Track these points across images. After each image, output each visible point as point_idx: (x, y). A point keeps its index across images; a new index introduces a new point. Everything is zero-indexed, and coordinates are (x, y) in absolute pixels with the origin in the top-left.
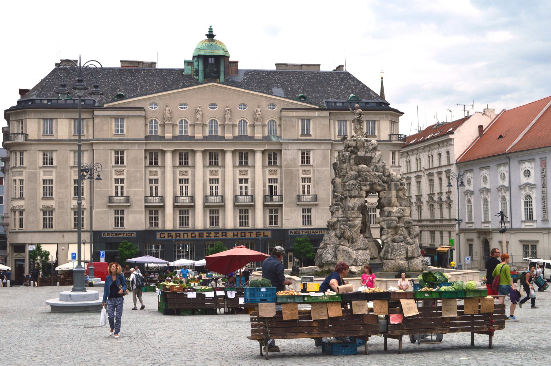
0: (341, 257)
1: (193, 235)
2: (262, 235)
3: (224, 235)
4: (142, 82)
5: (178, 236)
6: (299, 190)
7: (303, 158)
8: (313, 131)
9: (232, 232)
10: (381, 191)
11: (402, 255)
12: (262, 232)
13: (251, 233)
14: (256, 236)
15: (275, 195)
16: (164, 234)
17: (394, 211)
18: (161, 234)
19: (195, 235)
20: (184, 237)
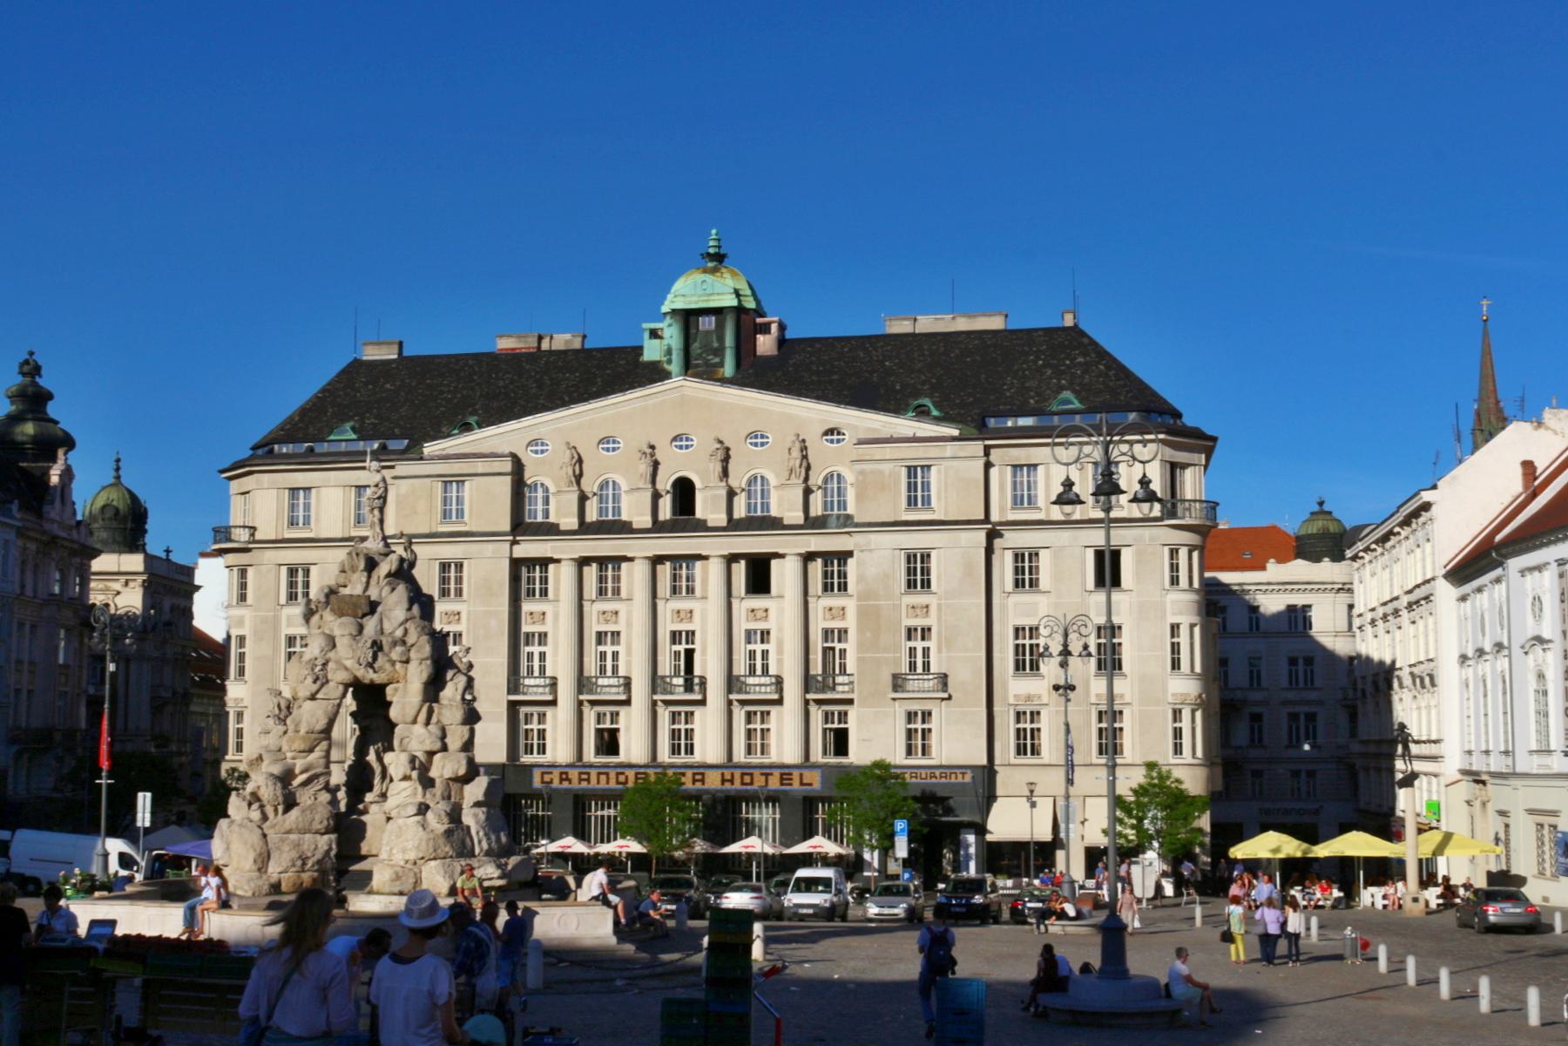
1: (622, 778)
2: (796, 785)
3: (698, 780)
4: (532, 388)
5: (584, 780)
6: (897, 661)
7: (911, 572)
8: (939, 499)
9: (720, 771)
12: (796, 773)
13: (767, 775)
14: (782, 784)
15: (840, 674)
16: (551, 773)
18: (543, 774)
19: (627, 777)
20: (598, 782)
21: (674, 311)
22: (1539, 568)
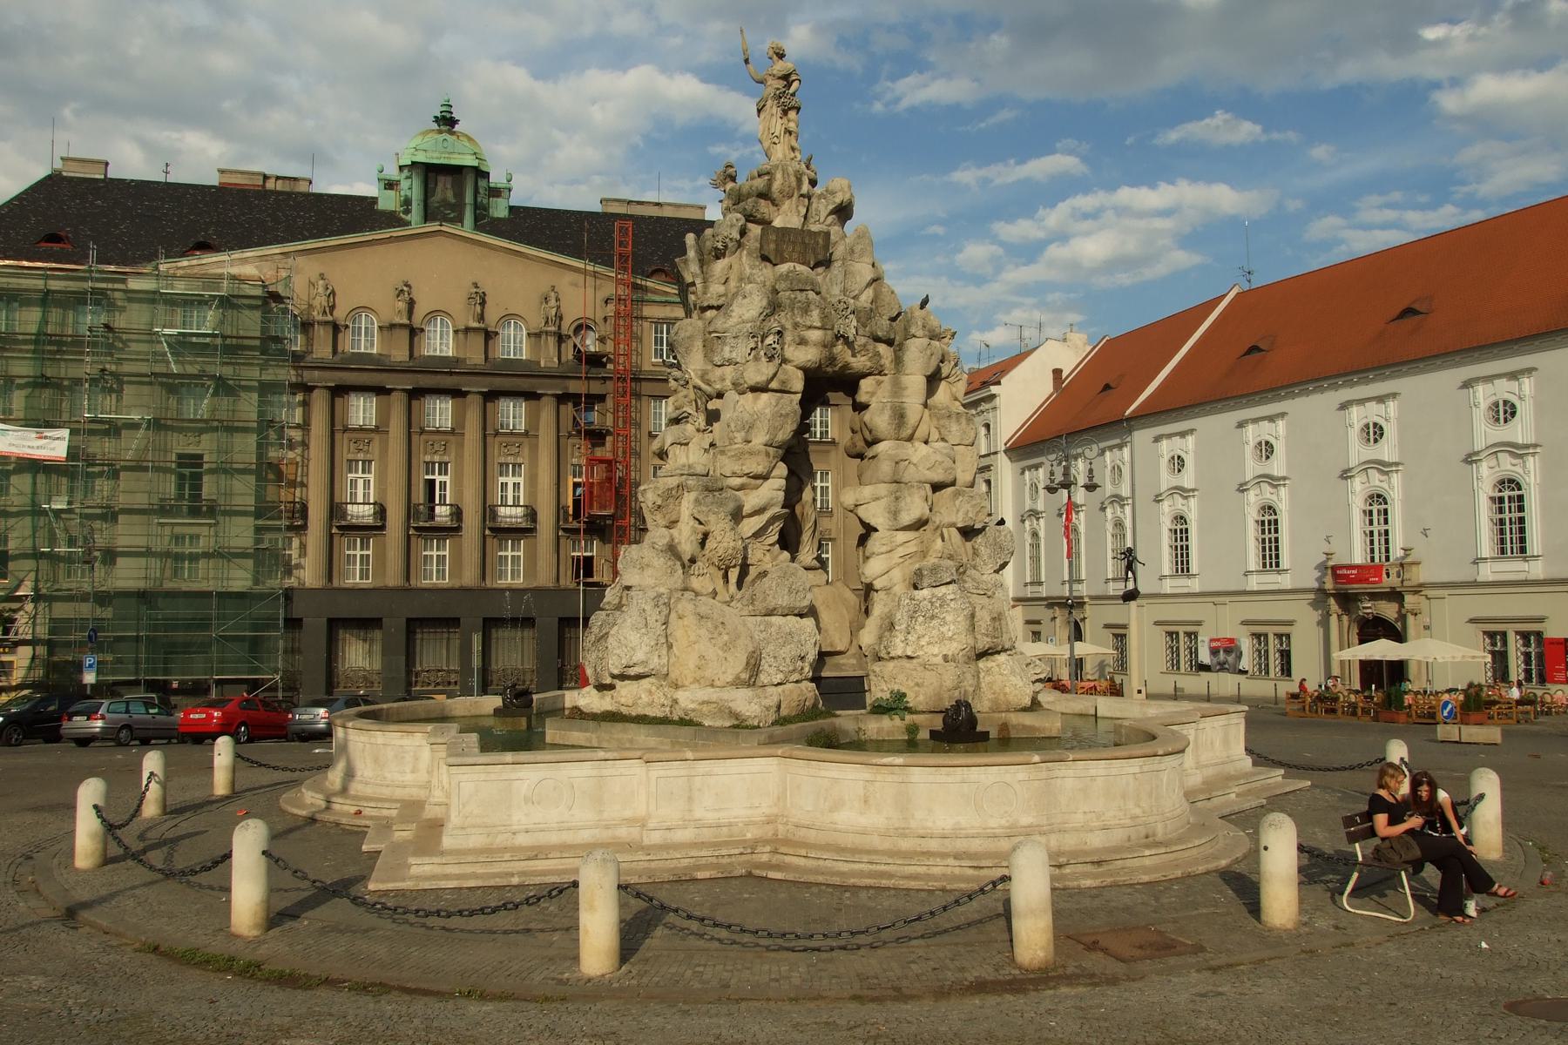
10: (865, 376)
11: (951, 639)
21: (414, 163)
22: (1183, 434)
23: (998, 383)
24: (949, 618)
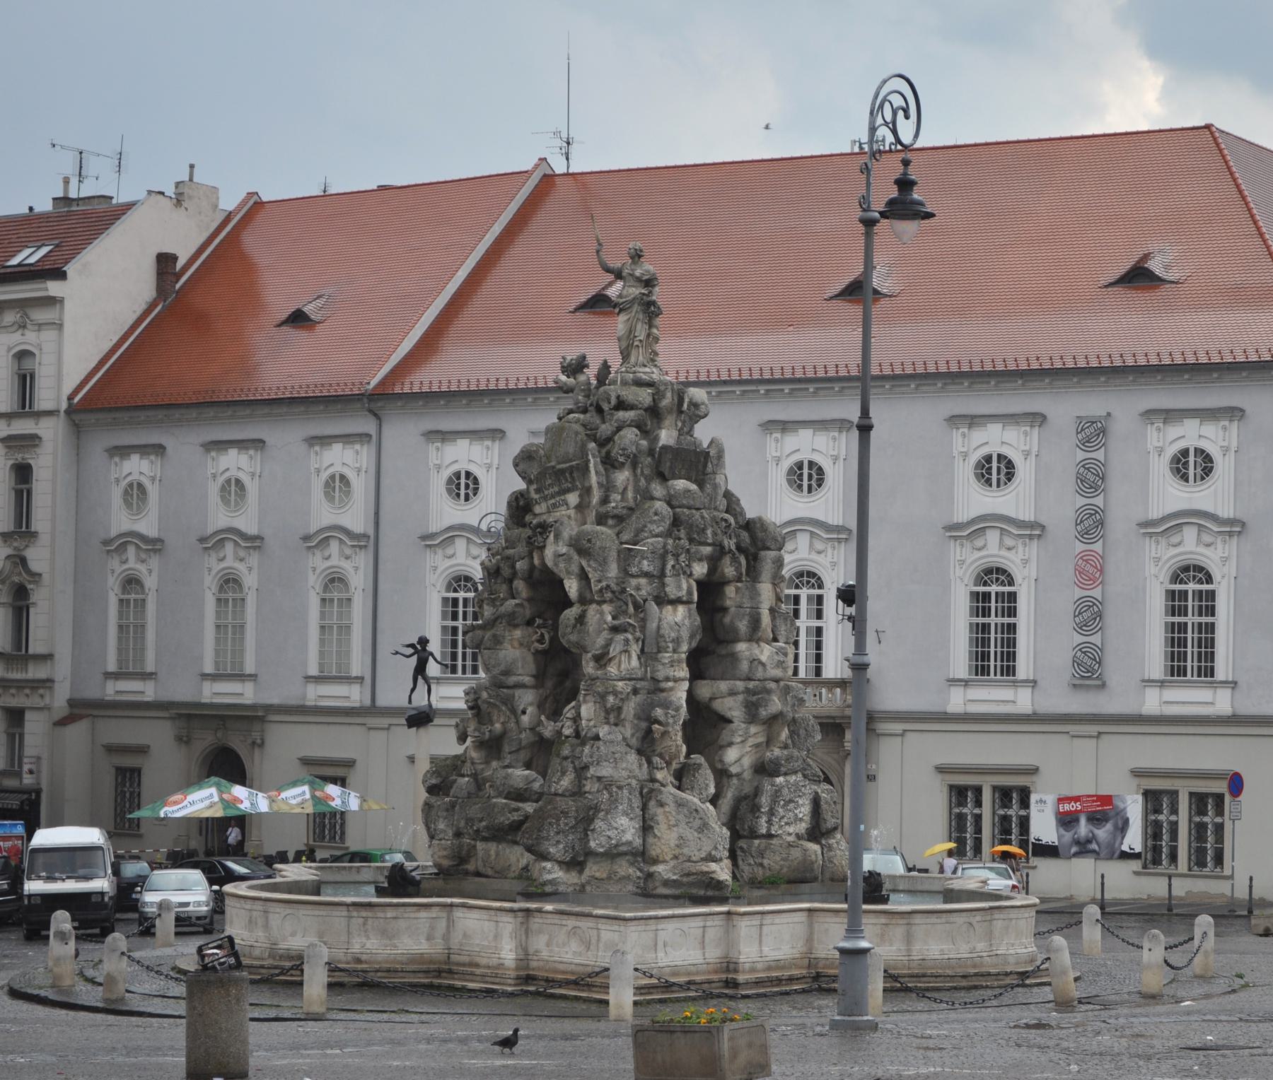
0: (670, 827)
11: (801, 820)
17: (764, 658)
23: (60, 275)
24: (800, 802)
